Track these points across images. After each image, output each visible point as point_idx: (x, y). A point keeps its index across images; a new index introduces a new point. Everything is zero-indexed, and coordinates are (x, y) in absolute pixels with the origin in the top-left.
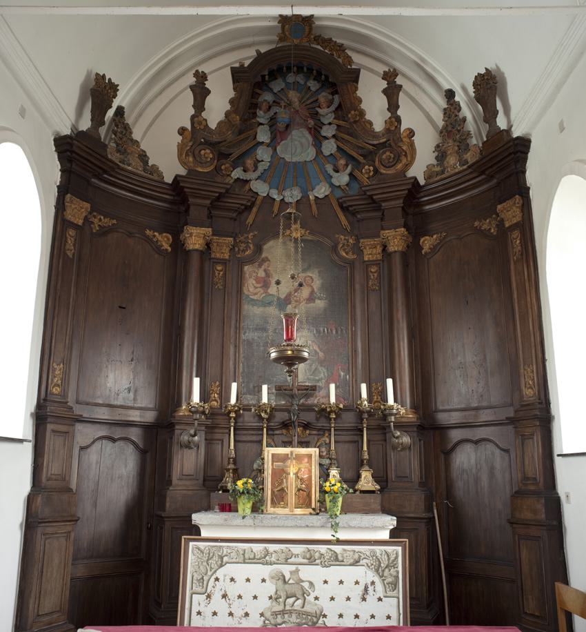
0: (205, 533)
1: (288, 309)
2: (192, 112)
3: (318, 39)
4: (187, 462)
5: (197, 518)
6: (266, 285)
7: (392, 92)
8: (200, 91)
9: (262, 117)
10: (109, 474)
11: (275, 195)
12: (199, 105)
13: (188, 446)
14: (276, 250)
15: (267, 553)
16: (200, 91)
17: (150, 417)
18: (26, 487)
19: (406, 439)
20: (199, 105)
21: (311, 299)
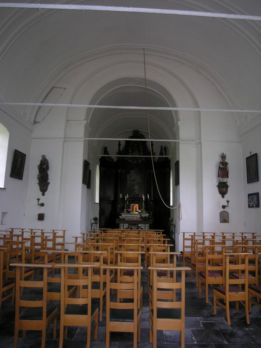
0: (122, 216)
1: (134, 178)
2: (118, 149)
3: (140, 134)
4: (119, 206)
5: (121, 214)
6: (131, 178)
7: (152, 145)
8: (119, 145)
9: (130, 148)
10: (108, 208)
11: (132, 162)
12: (119, 147)
13: (119, 203)
14: (132, 172)
15: (131, 218)
16: (119, 145)
17: (113, 199)
18: (99, 209)
19: (152, 203)
20: (119, 147)
21: (138, 180)
